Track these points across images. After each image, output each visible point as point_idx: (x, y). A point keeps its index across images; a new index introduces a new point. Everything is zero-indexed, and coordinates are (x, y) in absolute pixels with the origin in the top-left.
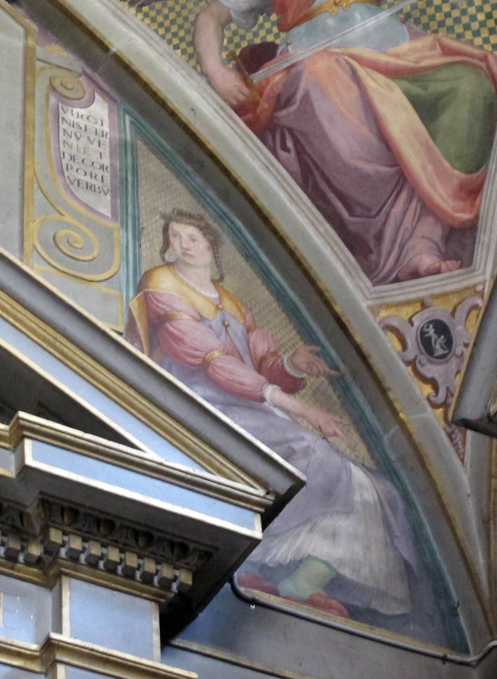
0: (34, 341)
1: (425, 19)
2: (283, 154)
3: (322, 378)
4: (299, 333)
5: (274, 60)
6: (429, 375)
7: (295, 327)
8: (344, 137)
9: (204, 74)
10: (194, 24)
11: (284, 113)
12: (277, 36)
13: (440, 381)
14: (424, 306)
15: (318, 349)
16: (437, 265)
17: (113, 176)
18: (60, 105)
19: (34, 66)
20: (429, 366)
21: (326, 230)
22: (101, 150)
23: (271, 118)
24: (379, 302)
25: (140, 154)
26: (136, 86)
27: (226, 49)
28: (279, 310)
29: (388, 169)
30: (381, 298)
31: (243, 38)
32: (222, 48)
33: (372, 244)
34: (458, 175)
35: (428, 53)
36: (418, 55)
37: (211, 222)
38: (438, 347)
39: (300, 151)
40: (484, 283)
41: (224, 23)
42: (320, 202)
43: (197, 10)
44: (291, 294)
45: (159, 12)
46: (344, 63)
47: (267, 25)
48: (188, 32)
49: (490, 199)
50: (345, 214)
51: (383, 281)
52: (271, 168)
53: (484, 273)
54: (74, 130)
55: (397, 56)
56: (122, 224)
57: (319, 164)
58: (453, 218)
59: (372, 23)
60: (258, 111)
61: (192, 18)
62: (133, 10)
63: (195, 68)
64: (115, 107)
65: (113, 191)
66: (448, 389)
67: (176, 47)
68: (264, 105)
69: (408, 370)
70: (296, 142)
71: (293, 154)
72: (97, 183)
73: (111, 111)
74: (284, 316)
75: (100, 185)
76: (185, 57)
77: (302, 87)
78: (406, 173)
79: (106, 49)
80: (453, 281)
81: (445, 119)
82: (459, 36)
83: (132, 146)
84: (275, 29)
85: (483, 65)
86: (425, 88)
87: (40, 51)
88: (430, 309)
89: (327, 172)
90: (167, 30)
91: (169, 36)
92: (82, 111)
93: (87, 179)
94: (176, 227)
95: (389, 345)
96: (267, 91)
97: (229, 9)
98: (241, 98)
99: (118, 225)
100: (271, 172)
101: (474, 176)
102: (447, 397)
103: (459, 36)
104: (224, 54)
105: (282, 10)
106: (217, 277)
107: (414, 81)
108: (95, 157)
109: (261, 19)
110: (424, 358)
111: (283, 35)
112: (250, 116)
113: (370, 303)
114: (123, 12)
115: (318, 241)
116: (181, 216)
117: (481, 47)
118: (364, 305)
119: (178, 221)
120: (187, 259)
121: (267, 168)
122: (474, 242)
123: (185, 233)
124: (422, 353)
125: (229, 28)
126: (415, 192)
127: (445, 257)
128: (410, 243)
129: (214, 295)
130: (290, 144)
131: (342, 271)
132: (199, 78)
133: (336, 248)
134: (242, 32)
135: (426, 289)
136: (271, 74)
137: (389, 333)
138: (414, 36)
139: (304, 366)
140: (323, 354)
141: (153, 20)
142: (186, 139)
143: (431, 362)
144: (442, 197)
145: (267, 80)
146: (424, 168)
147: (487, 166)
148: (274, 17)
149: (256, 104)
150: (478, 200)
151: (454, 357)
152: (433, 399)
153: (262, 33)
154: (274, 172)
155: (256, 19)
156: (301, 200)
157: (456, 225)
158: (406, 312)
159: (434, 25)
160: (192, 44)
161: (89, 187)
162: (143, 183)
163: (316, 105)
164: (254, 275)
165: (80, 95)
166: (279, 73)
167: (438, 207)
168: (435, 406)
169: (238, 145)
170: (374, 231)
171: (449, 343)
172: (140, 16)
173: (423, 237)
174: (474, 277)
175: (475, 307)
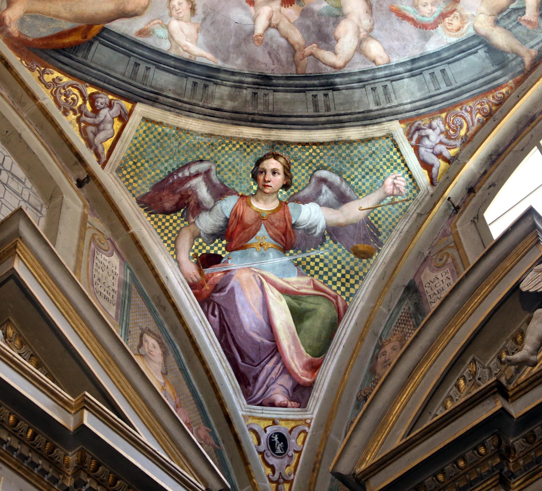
0: (95, 357)
1: (308, 267)
2: (212, 317)
3: (211, 447)
4: (202, 418)
5: (219, 265)
6: (271, 463)
7: (200, 414)
8: (249, 317)
9: (177, 261)
10: (178, 232)
11: (217, 295)
12: (224, 252)
13: (277, 468)
14: (274, 423)
15: (210, 430)
16: (286, 402)
17: (118, 297)
18: (96, 250)
19: (86, 224)
20: (271, 457)
21: (227, 366)
22: (114, 281)
23: (209, 296)
24: (249, 414)
25: (133, 292)
26: (138, 254)
27: (193, 251)
28: (193, 402)
29: (269, 342)
30: (251, 412)
31: (204, 248)
32: (191, 250)
33: (251, 381)
34: (308, 357)
35: (306, 286)
36: (299, 285)
37: (164, 341)
38: (278, 448)
39: (222, 318)
40: (311, 419)
41: (196, 236)
42: (227, 350)
43: (182, 225)
44: (200, 395)
45: (160, 220)
46: (258, 278)
47: (220, 245)
48: (174, 235)
49: (323, 374)
50: (240, 360)
51: (253, 403)
52: (203, 323)
53: (312, 414)
54: (101, 265)
55: (288, 283)
56: (120, 324)
57: (231, 329)
58: (301, 379)
59: (278, 261)
60: (203, 290)
61: (178, 229)
62: (146, 214)
63: (173, 256)
64: (123, 263)
65: (118, 305)
66: (280, 473)
67: (165, 242)
68: (207, 287)
69: (259, 457)
70: (221, 312)
71: (217, 319)
72: (110, 298)
73: (120, 264)
74: (195, 406)
75: (112, 299)
76: (169, 249)
77: (232, 283)
78: (278, 347)
79: (127, 228)
80: (294, 413)
81: (307, 324)
82: (325, 282)
83: (129, 286)
84: (224, 249)
85: (334, 301)
86: (300, 304)
87: (90, 218)
88: (277, 426)
89: (234, 334)
90: (162, 231)
91: (162, 234)
92: (106, 258)
93: (105, 293)
94: (147, 337)
95: (251, 440)
96: (211, 280)
97: (200, 230)
98: (196, 280)
99: (118, 324)
100: (202, 325)
101: (317, 359)
102: (279, 478)
103: (325, 282)
104: (192, 254)
105: (230, 239)
106: (165, 372)
107: (294, 299)
108: (110, 284)
109: (217, 241)
110: (269, 453)
111: (227, 253)
112: (197, 291)
113: (244, 413)
114: (140, 214)
115: (222, 371)
116: (150, 332)
117: (335, 291)
118: (240, 413)
119: (148, 334)
120: (150, 356)
121: (201, 322)
122: (310, 396)
123: (151, 342)
124: (269, 450)
125: (198, 241)
126: (281, 359)
127: (291, 399)
128: (273, 386)
129: (162, 381)
130: (217, 313)
131: (231, 391)
132: (173, 262)
133: (230, 377)
134: (204, 244)
135: (277, 414)
136: (215, 272)
137: (252, 433)
138: (300, 274)
139: (203, 437)
140: (212, 433)
141: (156, 223)
142: (160, 292)
143: (273, 456)
144: (296, 365)
145: (213, 274)
146: (289, 347)
147: (325, 357)
148: (224, 242)
149: (203, 286)
150: (316, 373)
151: (287, 456)
152: (271, 477)
153: (216, 248)
154: (204, 325)
155: (214, 240)
156: (216, 345)
157: (301, 383)
158: (264, 424)
159: (312, 272)
160: (174, 242)
161: (105, 297)
162: (132, 307)
163: (237, 296)
164: (182, 378)
165: (106, 248)
166: (220, 272)
167: (293, 370)
168: (271, 481)
169: (188, 305)
170: (253, 374)
171: (285, 447)
172: (149, 219)
173: (282, 385)
174: (307, 414)
175: (304, 431)
